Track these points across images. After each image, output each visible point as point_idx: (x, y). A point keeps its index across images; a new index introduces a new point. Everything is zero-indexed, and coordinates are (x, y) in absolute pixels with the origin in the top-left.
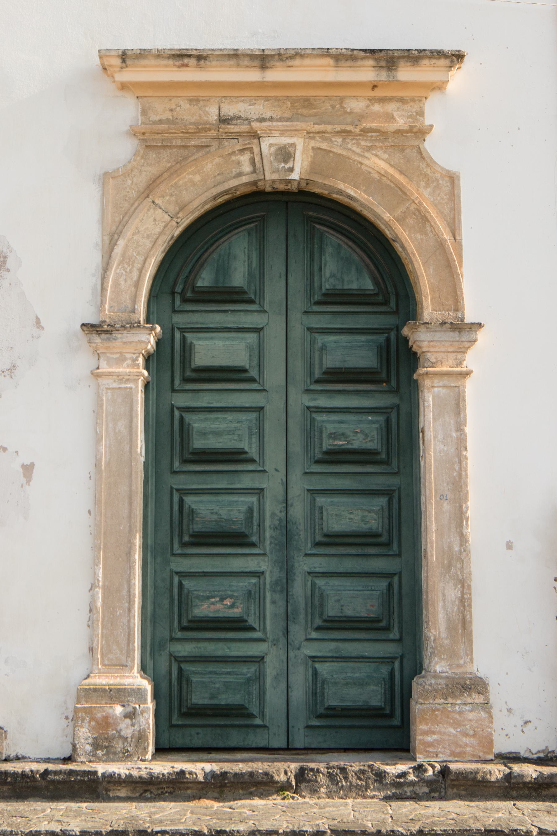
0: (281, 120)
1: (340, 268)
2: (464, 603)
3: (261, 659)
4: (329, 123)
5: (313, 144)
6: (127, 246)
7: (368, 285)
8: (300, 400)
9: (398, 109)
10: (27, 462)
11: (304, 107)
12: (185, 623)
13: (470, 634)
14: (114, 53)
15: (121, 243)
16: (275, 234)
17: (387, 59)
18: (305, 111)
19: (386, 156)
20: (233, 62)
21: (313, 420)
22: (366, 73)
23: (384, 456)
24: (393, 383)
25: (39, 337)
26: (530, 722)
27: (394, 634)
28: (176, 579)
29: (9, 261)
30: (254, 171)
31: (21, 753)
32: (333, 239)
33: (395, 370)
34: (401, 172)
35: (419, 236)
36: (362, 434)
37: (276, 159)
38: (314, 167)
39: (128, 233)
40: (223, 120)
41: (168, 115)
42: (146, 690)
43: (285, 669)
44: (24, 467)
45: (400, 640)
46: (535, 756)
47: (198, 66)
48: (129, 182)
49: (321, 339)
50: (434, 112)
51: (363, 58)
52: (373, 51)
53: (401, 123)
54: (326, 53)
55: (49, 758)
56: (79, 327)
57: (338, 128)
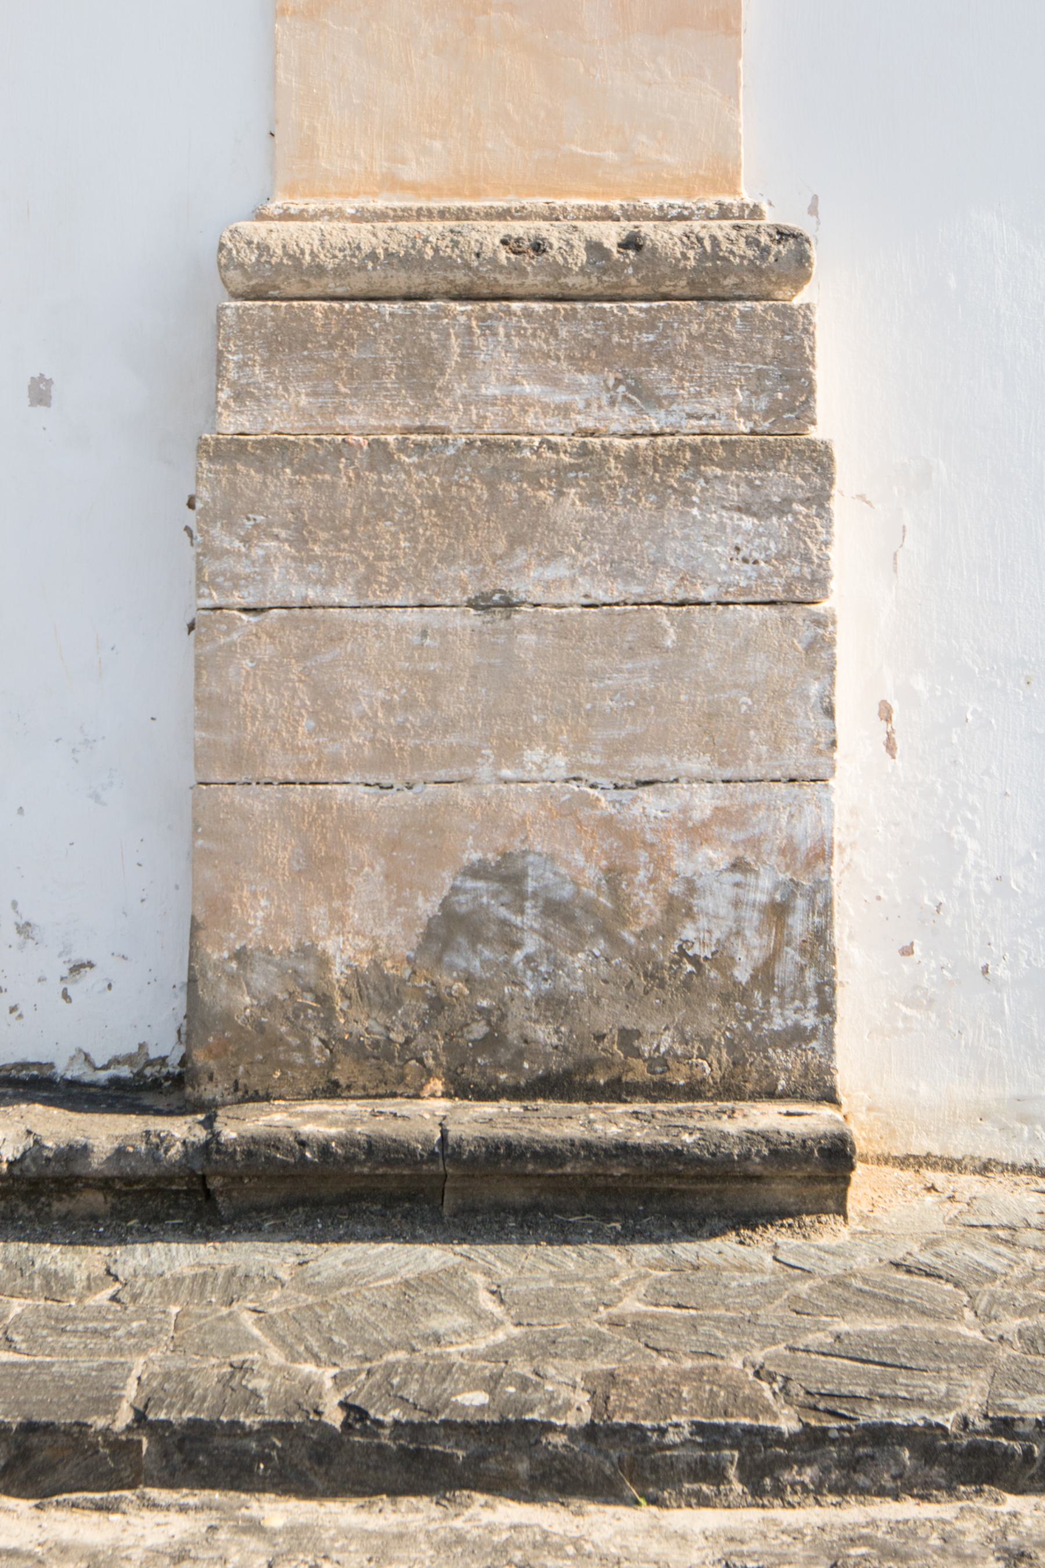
26: (90, 965)
46: (103, 1076)
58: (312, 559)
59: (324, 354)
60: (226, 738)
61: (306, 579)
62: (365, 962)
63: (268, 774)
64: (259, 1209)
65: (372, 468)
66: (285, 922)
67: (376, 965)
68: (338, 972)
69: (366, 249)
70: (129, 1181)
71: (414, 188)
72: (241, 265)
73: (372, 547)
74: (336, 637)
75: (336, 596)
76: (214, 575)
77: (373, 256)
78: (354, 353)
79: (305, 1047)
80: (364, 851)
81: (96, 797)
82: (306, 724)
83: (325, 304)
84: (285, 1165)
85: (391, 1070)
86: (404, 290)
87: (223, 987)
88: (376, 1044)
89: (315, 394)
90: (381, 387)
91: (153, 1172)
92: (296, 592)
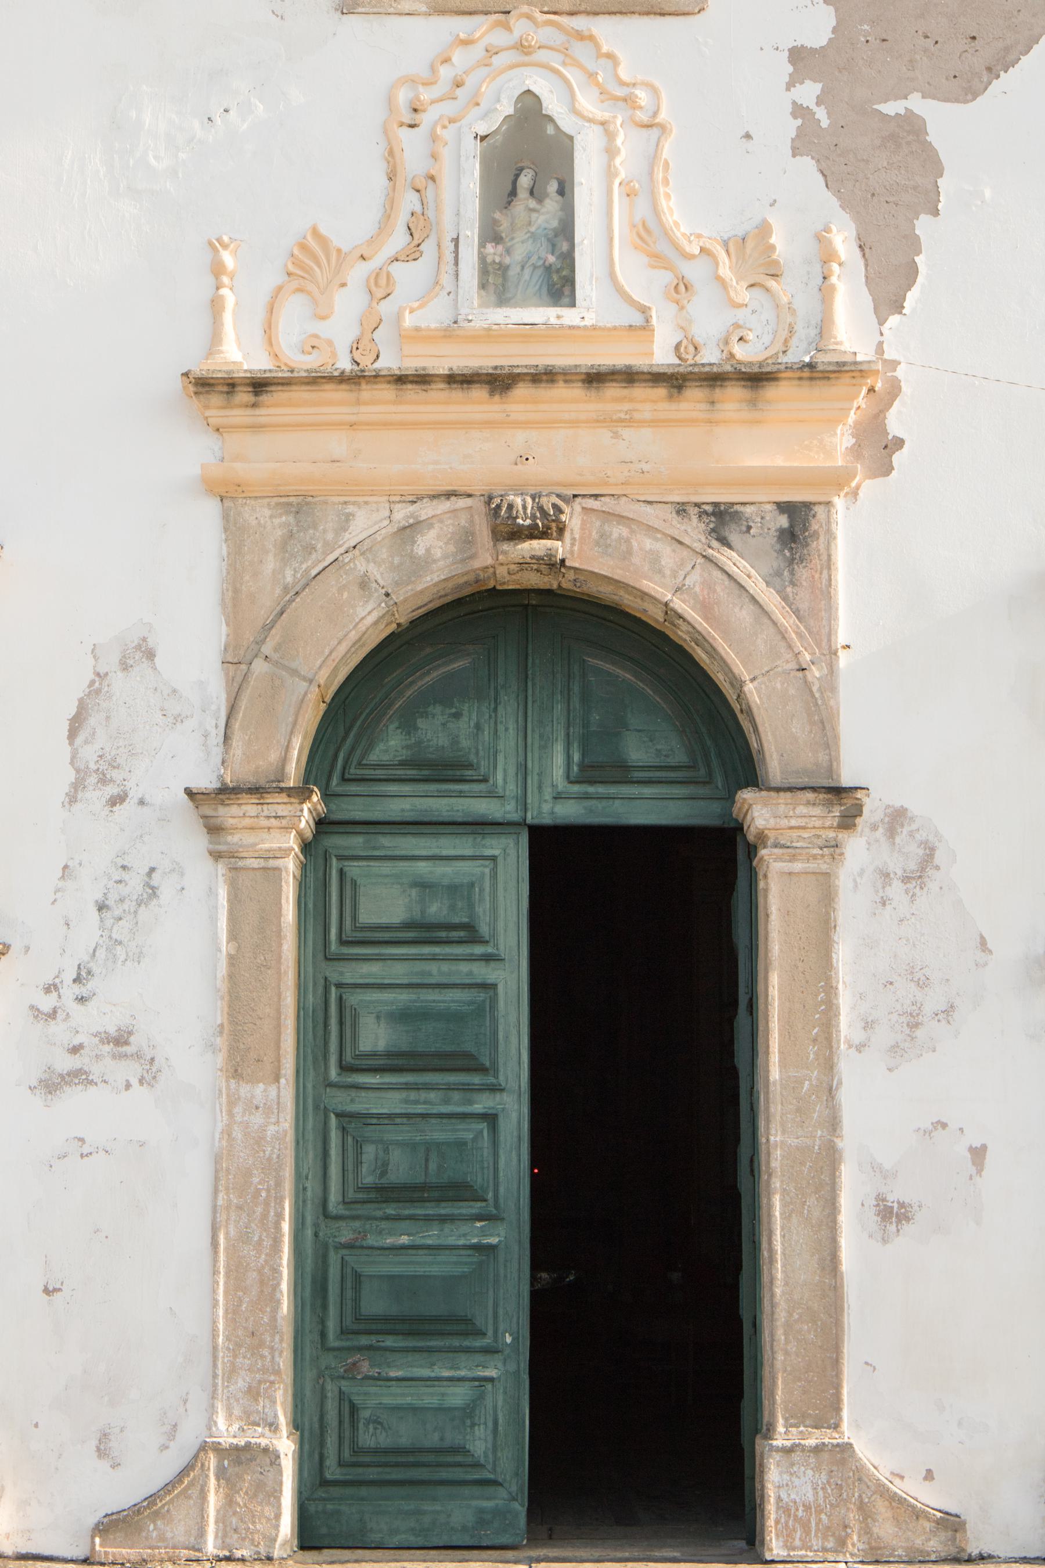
10: (977, 1144)
25: (986, 964)
29: (937, 854)
31: (986, 1550)
44: (973, 1150)
55: (1025, 1558)
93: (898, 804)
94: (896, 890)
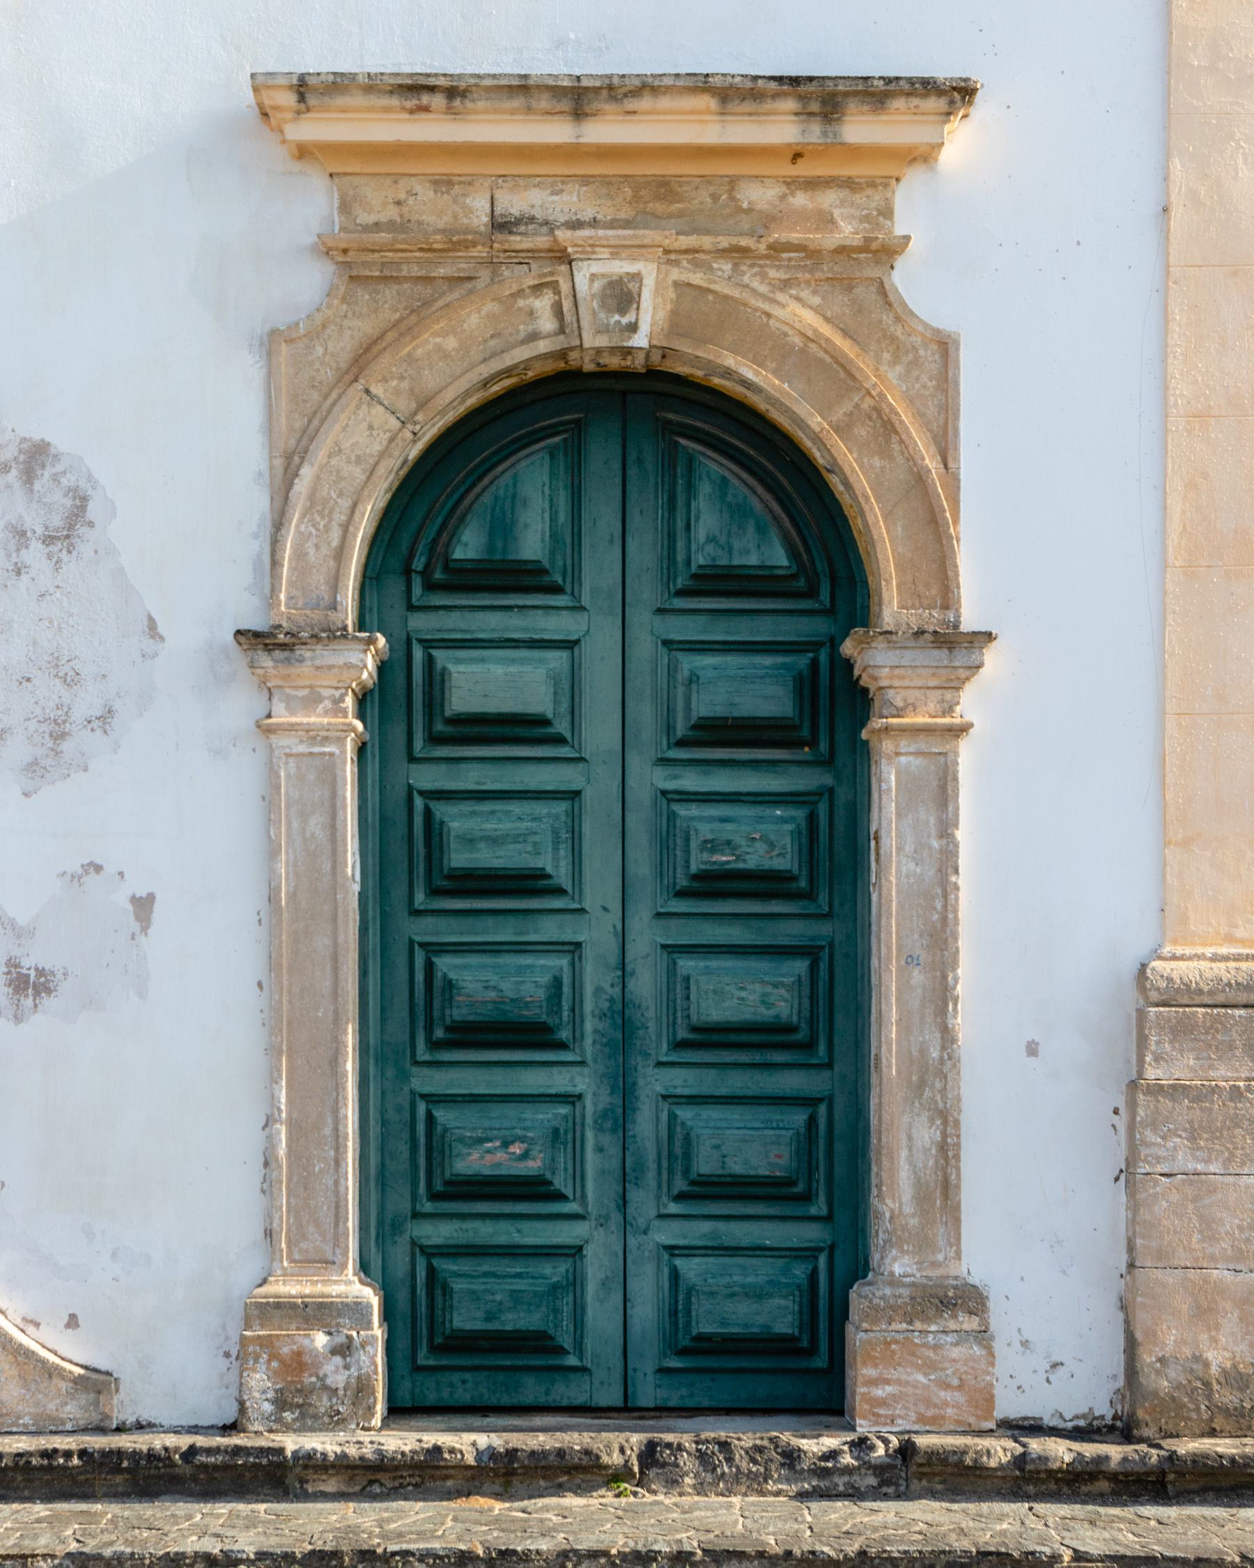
0: (612, 224)
1: (725, 524)
2: (947, 1151)
3: (575, 1252)
4: (707, 232)
5: (675, 274)
6: (318, 478)
7: (779, 557)
8: (649, 778)
9: (842, 203)
10: (142, 892)
11: (658, 198)
12: (439, 1187)
13: (957, 1208)
14: (282, 81)
15: (307, 472)
16: (602, 457)
17: (823, 98)
18: (659, 207)
19: (816, 300)
20: (518, 102)
21: (672, 816)
22: (781, 128)
23: (803, 883)
24: (823, 747)
25: (155, 655)
26: (1062, 1364)
27: (819, 1207)
28: (422, 1108)
29: (91, 505)
30: (562, 330)
31: (146, 1416)
32: (713, 466)
33: (829, 719)
34: (846, 333)
35: (877, 462)
36: (765, 842)
37: (603, 305)
38: (677, 323)
39: (320, 453)
40: (502, 225)
41: (391, 213)
42: (369, 1306)
43: (621, 1270)
44: (135, 900)
45: (828, 1219)
46: (1070, 1425)
47: (450, 111)
48: (320, 350)
49: (689, 663)
50: (913, 210)
51: (776, 96)
52: (795, 81)
53: (847, 231)
54: (701, 84)
55: (196, 1426)
56: (230, 637)
57: (725, 242)
58: (1200, 1148)
59: (1202, 1037)
60: (1154, 1244)
61: (1196, 1159)
62: (1228, 1365)
63: (1176, 1263)
64: (1189, 1492)
65: (1231, 1100)
66: (1185, 1343)
67: (1235, 1366)
68: (1214, 1370)
69: (1225, 980)
70: (1126, 1474)
71: (1243, 942)
72: (1158, 989)
73: (1232, 1143)
74: (1213, 1190)
75: (1212, 1169)
76: (1146, 1156)
77: (1229, 984)
78: (1219, 1037)
79: (1198, 1409)
80: (1228, 1306)
81: (1064, 1272)
82: (1196, 1237)
83: (1203, 1010)
84: (1213, 1467)
85: (1244, 1422)
86: (1245, 1002)
87: (1153, 1377)
88: (1235, 1409)
89: (1198, 1059)
90: (1234, 1056)
91: (1143, 1469)
92: (1191, 1166)
93: (37, 437)
94: (35, 554)
